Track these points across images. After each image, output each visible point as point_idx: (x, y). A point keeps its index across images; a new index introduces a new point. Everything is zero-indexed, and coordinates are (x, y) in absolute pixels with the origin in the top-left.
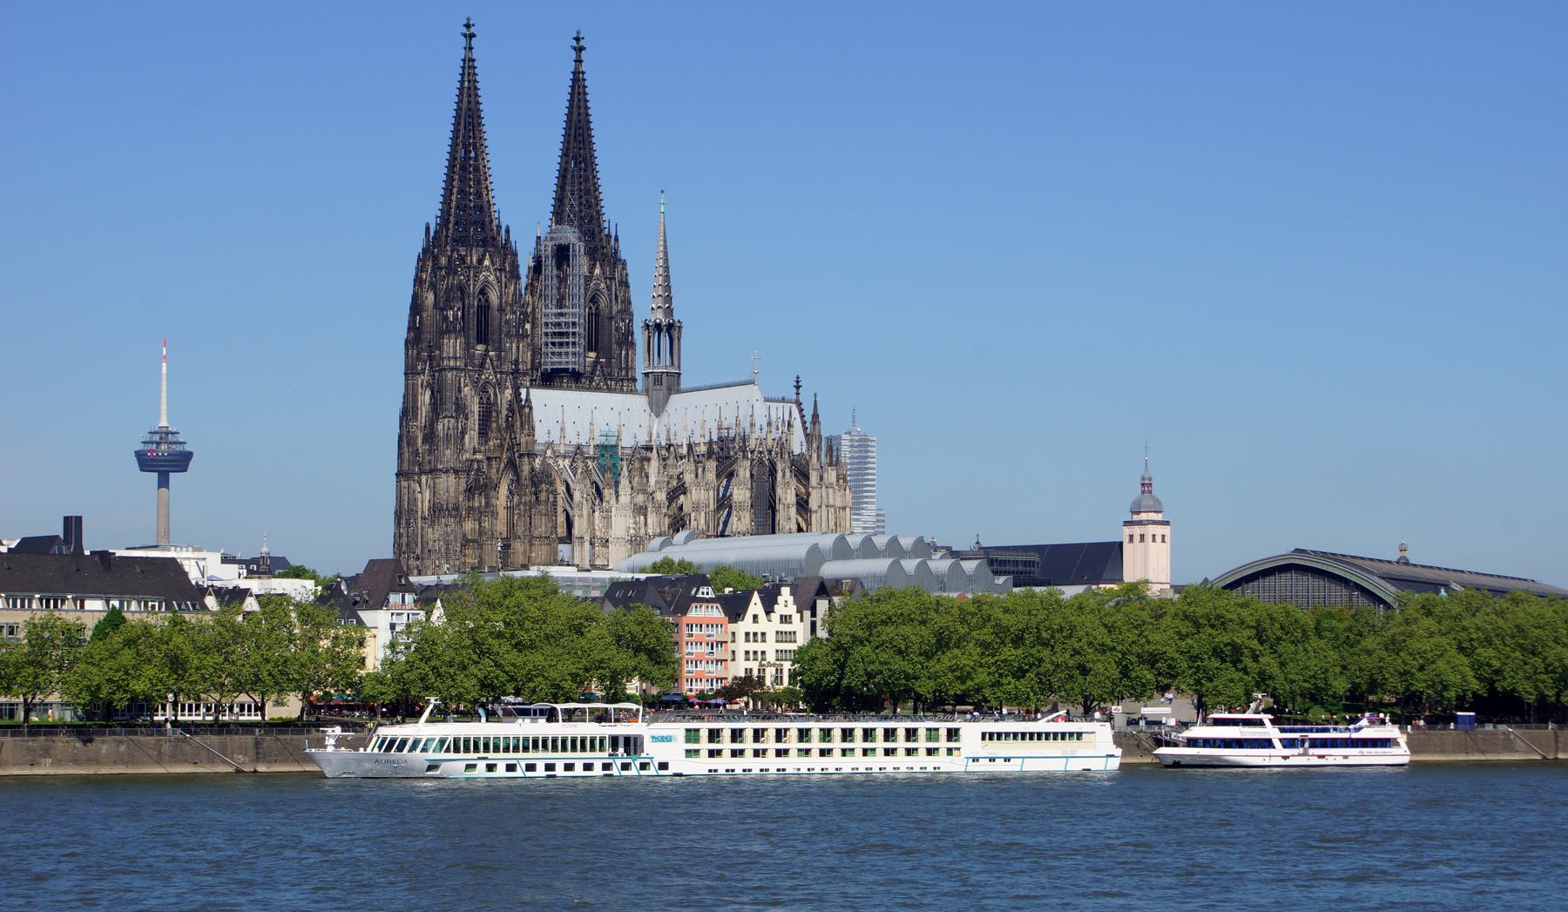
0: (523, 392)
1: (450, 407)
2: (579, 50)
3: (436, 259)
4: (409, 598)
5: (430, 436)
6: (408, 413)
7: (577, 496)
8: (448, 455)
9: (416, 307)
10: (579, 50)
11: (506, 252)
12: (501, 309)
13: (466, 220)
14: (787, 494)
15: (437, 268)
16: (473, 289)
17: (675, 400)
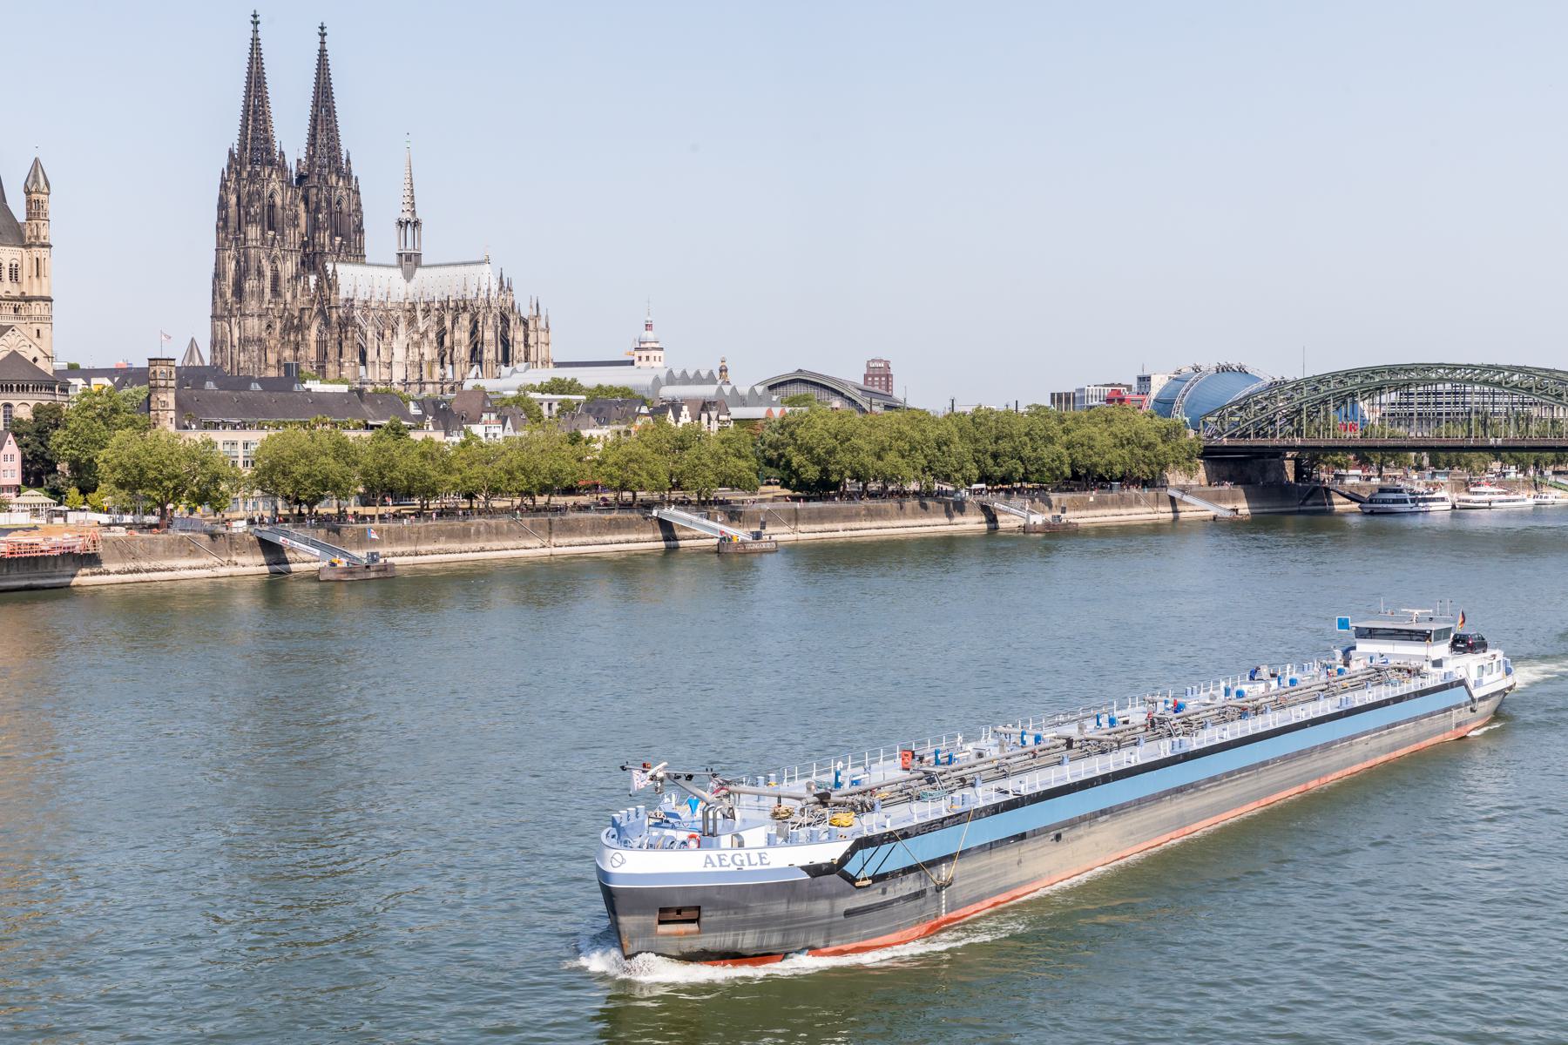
0: (330, 267)
1: (253, 271)
2: (323, 35)
3: (239, 174)
4: (493, 416)
5: (238, 291)
6: (218, 275)
7: (369, 335)
8: (252, 305)
9: (223, 205)
10: (323, 35)
11: (282, 168)
12: (283, 208)
13: (255, 144)
14: (517, 335)
15: (238, 180)
16: (266, 194)
17: (418, 270)
